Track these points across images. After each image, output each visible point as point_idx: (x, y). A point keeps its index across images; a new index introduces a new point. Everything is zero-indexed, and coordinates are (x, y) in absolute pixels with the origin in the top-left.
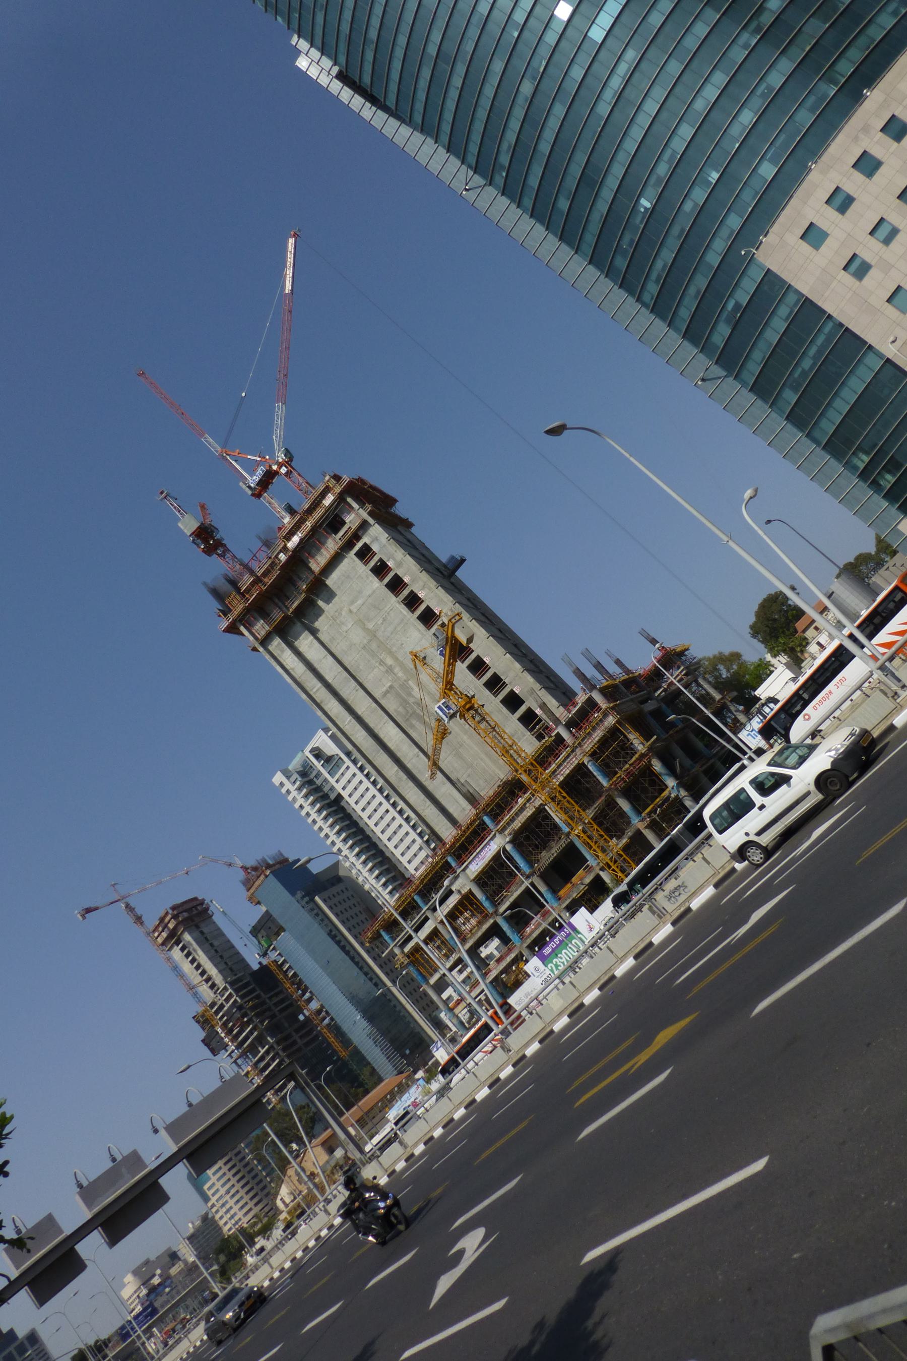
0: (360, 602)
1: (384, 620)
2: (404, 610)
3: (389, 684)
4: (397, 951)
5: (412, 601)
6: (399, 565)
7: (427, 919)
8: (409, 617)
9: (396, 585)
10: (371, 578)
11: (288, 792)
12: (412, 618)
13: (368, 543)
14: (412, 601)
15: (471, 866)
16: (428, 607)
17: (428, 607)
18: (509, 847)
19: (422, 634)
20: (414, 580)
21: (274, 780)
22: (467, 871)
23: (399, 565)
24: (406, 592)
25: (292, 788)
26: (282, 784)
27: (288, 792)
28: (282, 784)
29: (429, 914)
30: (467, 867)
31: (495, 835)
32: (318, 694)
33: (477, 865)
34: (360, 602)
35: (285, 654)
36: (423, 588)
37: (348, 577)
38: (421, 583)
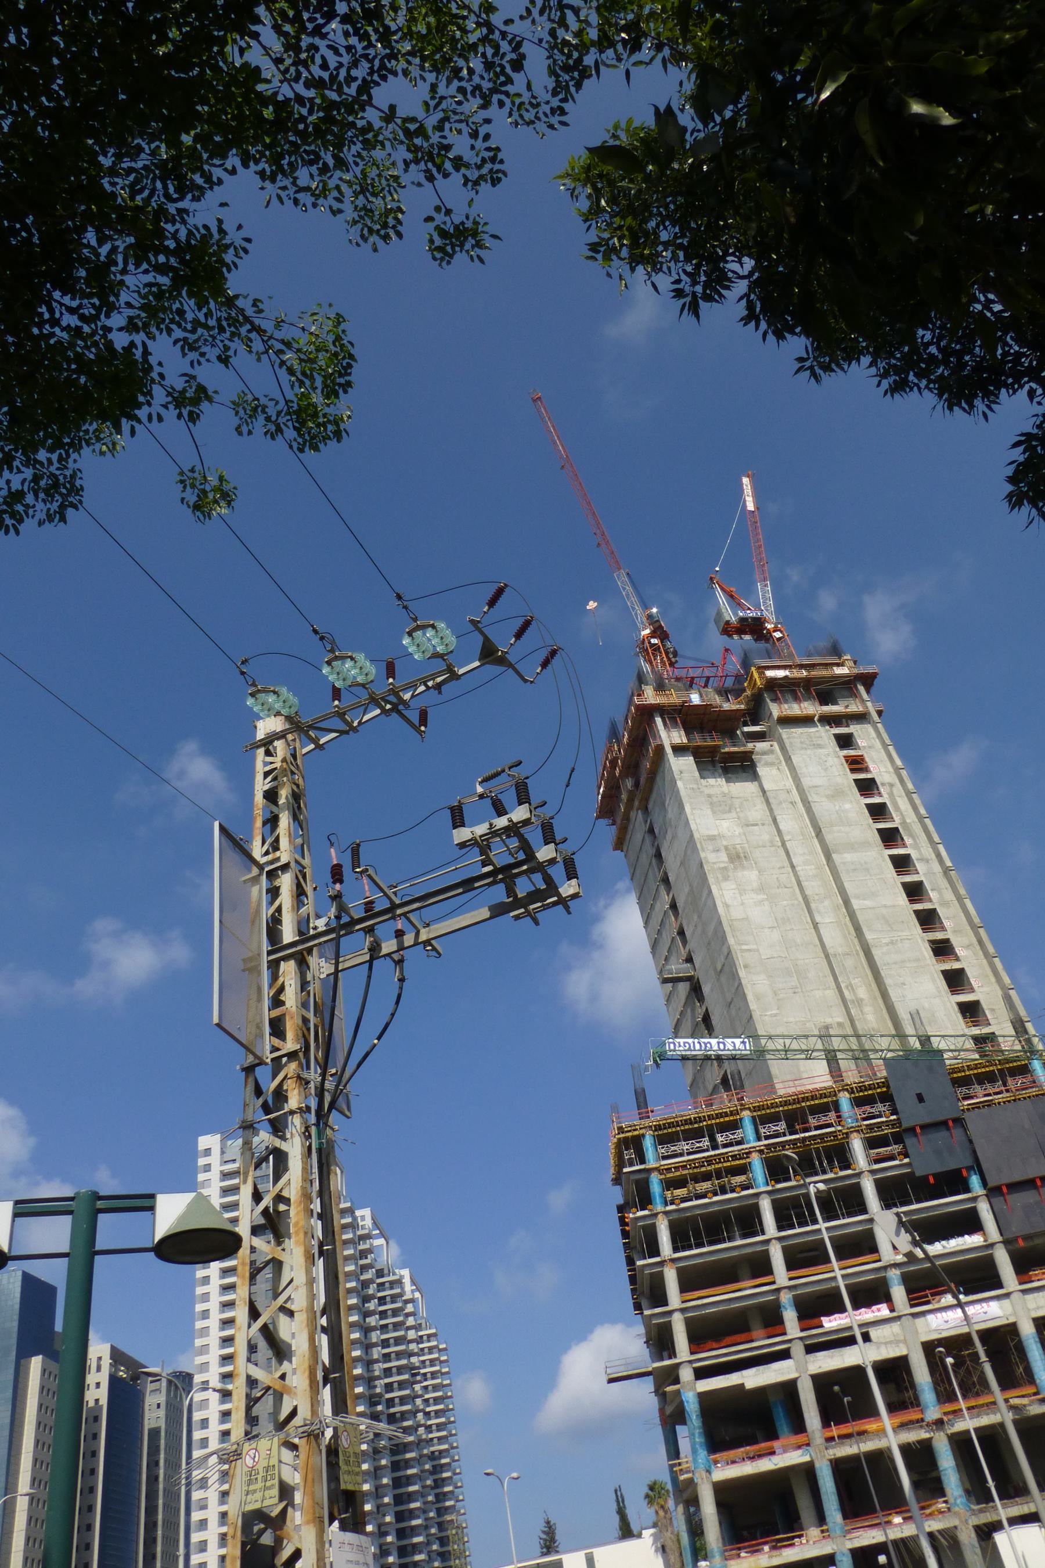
0: (868, 903)
1: (892, 943)
2: (927, 952)
3: (840, 1020)
4: (686, 1374)
5: (942, 949)
6: (945, 904)
7: (785, 1355)
8: (929, 962)
9: (928, 919)
10: (897, 891)
11: (207, 1168)
12: (935, 967)
13: (914, 856)
14: (942, 949)
15: (930, 1317)
16: (961, 972)
17: (961, 972)
18: (1027, 1330)
19: (939, 992)
20: (954, 932)
21: (200, 1139)
22: (920, 1322)
23: (945, 904)
24: (939, 936)
25: (217, 1168)
26: (208, 1152)
27: (207, 1168)
28: (208, 1152)
29: (797, 1349)
30: (923, 1314)
31: (1007, 1295)
32: (747, 955)
33: (945, 1320)
34: (868, 903)
35: (728, 883)
36: (967, 947)
37: (867, 870)
38: (966, 942)
